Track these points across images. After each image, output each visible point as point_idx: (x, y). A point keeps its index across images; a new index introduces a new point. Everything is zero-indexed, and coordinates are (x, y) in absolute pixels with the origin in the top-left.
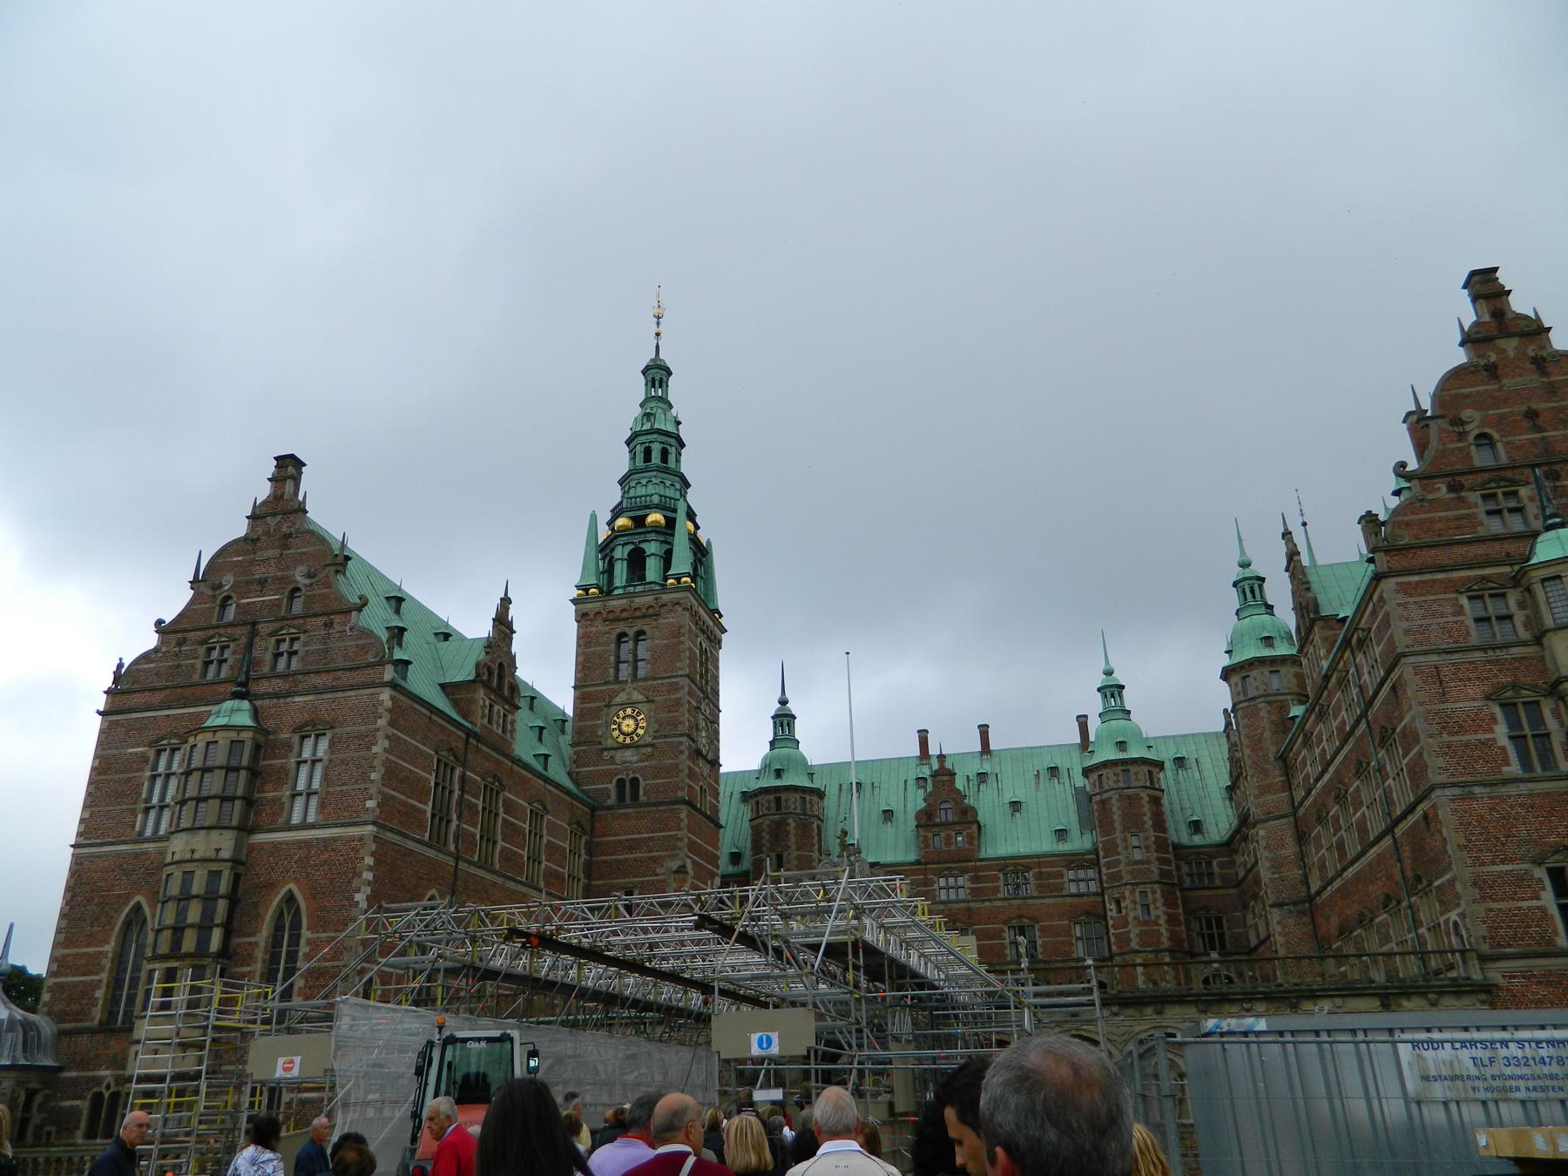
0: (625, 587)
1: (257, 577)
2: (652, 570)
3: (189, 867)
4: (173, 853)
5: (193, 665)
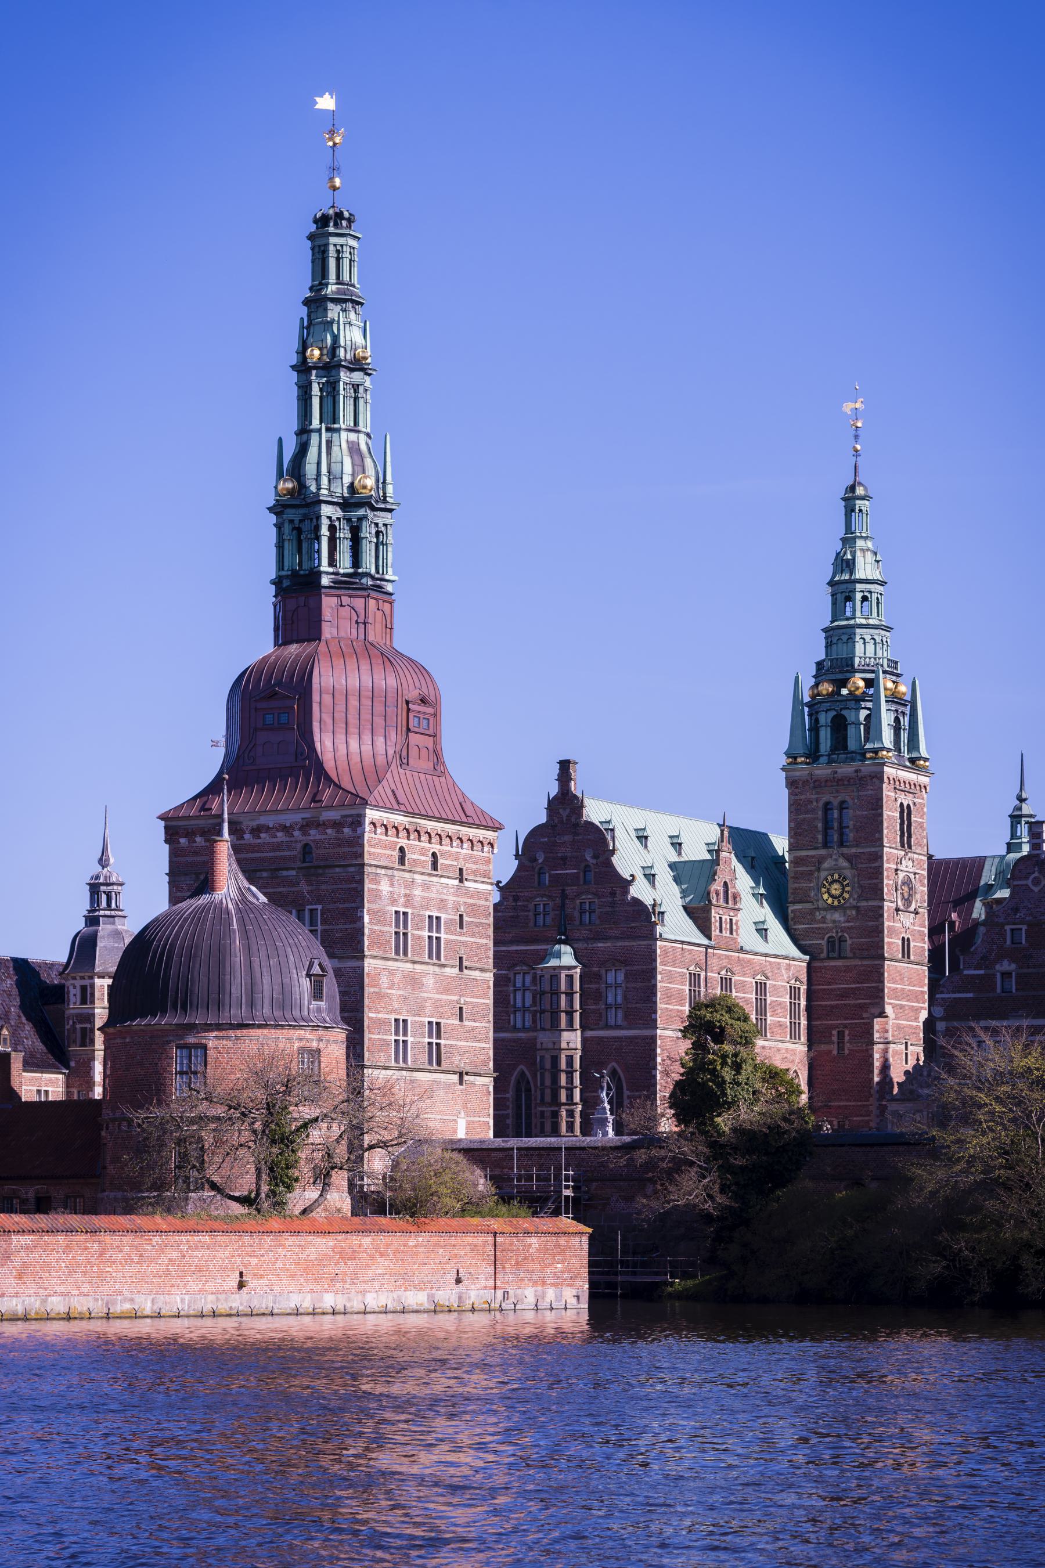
0: (829, 755)
1: (559, 855)
3: (554, 1053)
4: (542, 1043)
5: (527, 916)
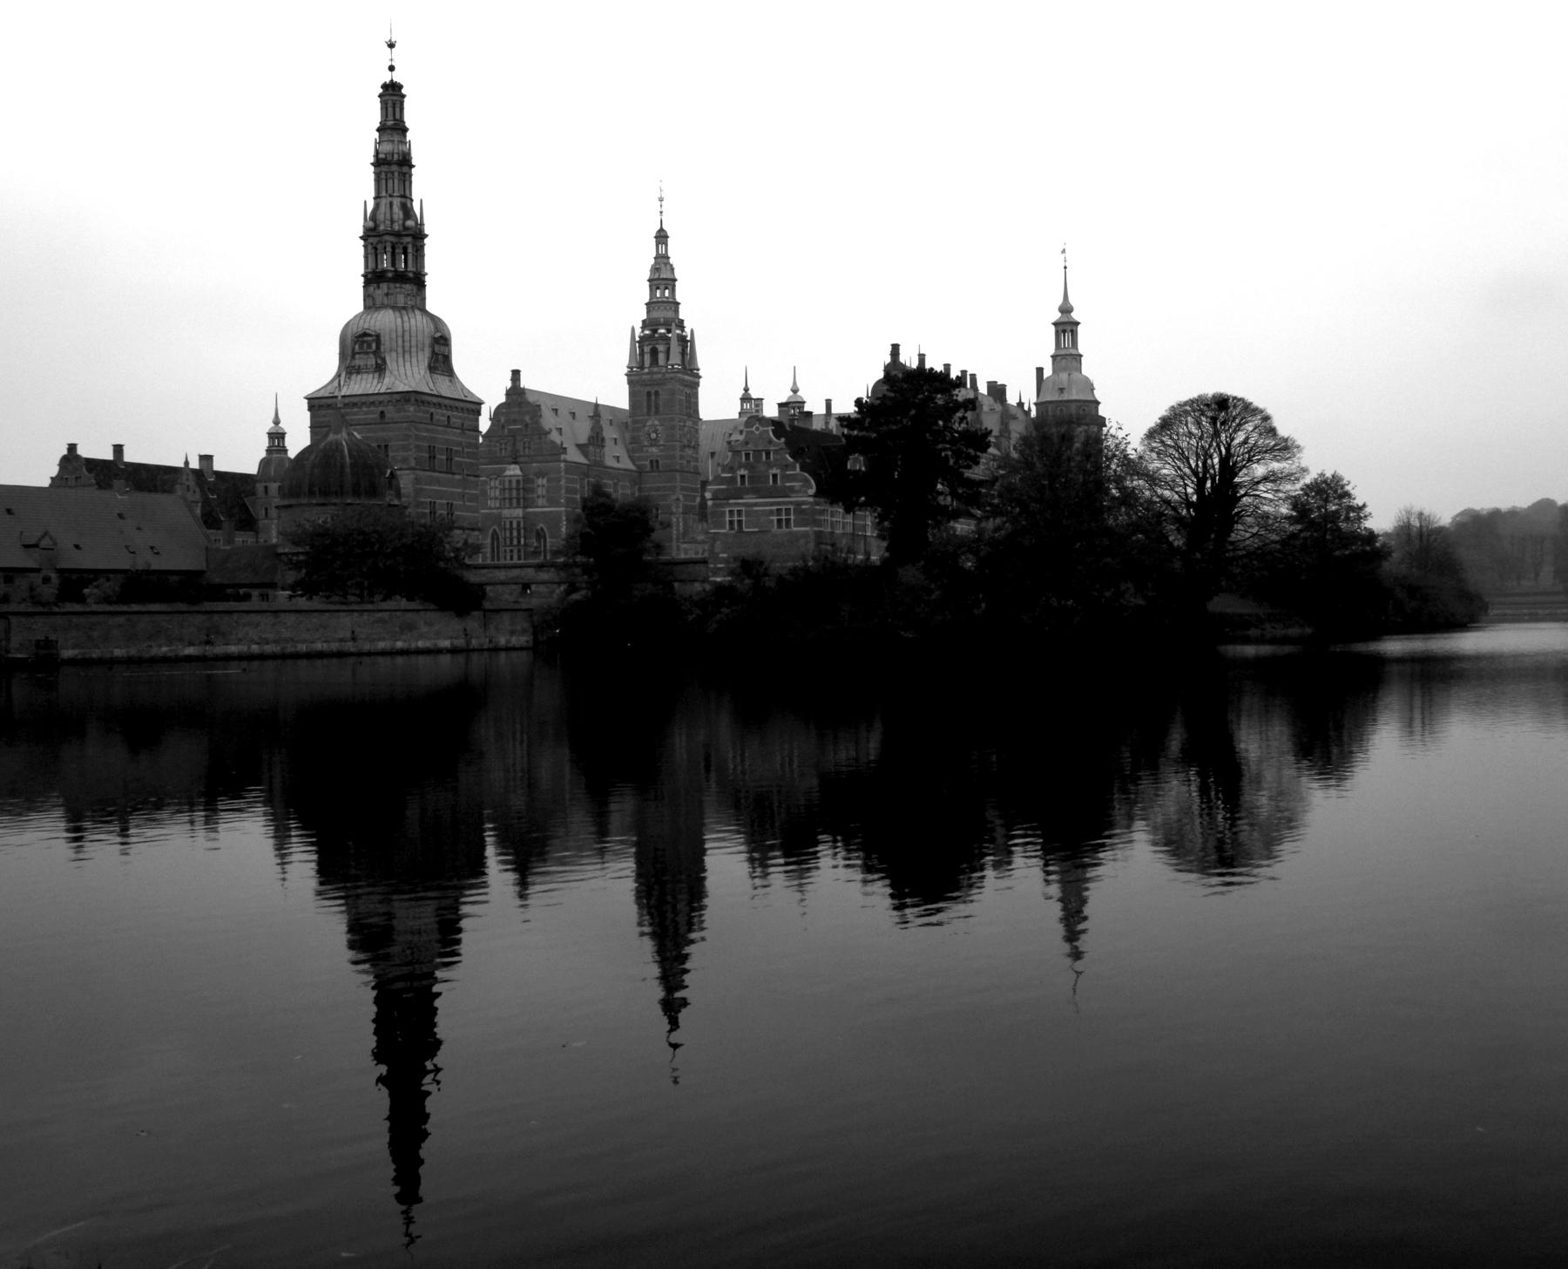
0: (649, 367)
2: (661, 360)
